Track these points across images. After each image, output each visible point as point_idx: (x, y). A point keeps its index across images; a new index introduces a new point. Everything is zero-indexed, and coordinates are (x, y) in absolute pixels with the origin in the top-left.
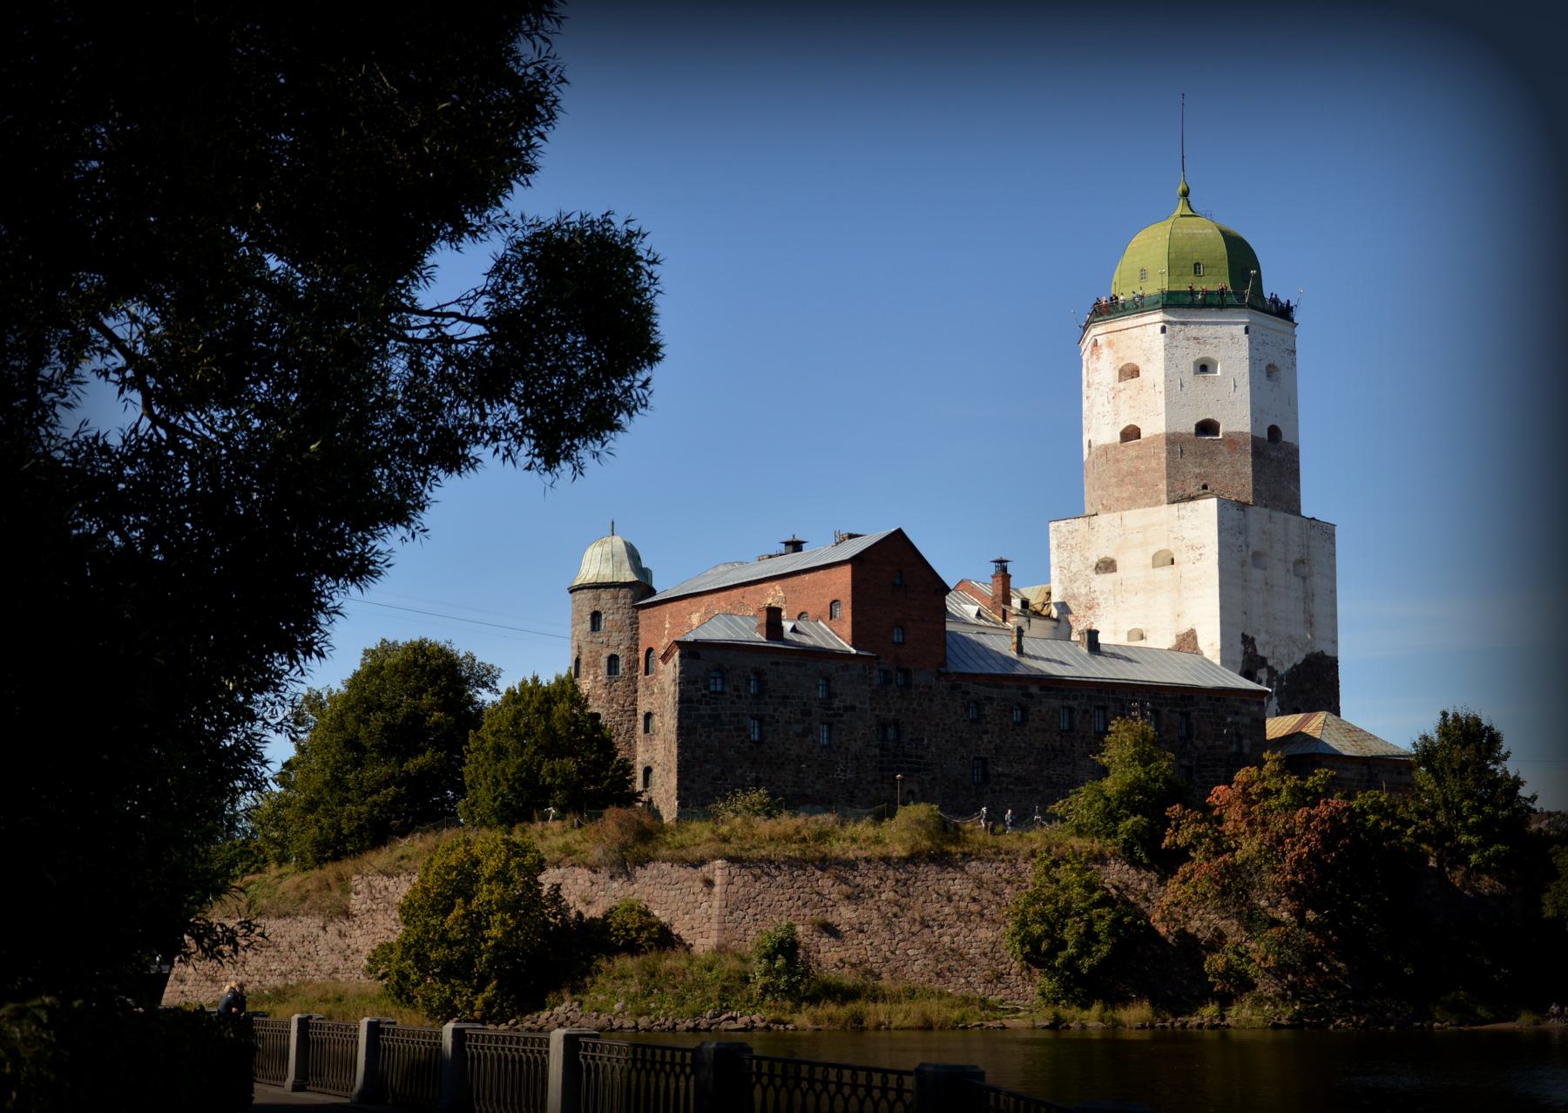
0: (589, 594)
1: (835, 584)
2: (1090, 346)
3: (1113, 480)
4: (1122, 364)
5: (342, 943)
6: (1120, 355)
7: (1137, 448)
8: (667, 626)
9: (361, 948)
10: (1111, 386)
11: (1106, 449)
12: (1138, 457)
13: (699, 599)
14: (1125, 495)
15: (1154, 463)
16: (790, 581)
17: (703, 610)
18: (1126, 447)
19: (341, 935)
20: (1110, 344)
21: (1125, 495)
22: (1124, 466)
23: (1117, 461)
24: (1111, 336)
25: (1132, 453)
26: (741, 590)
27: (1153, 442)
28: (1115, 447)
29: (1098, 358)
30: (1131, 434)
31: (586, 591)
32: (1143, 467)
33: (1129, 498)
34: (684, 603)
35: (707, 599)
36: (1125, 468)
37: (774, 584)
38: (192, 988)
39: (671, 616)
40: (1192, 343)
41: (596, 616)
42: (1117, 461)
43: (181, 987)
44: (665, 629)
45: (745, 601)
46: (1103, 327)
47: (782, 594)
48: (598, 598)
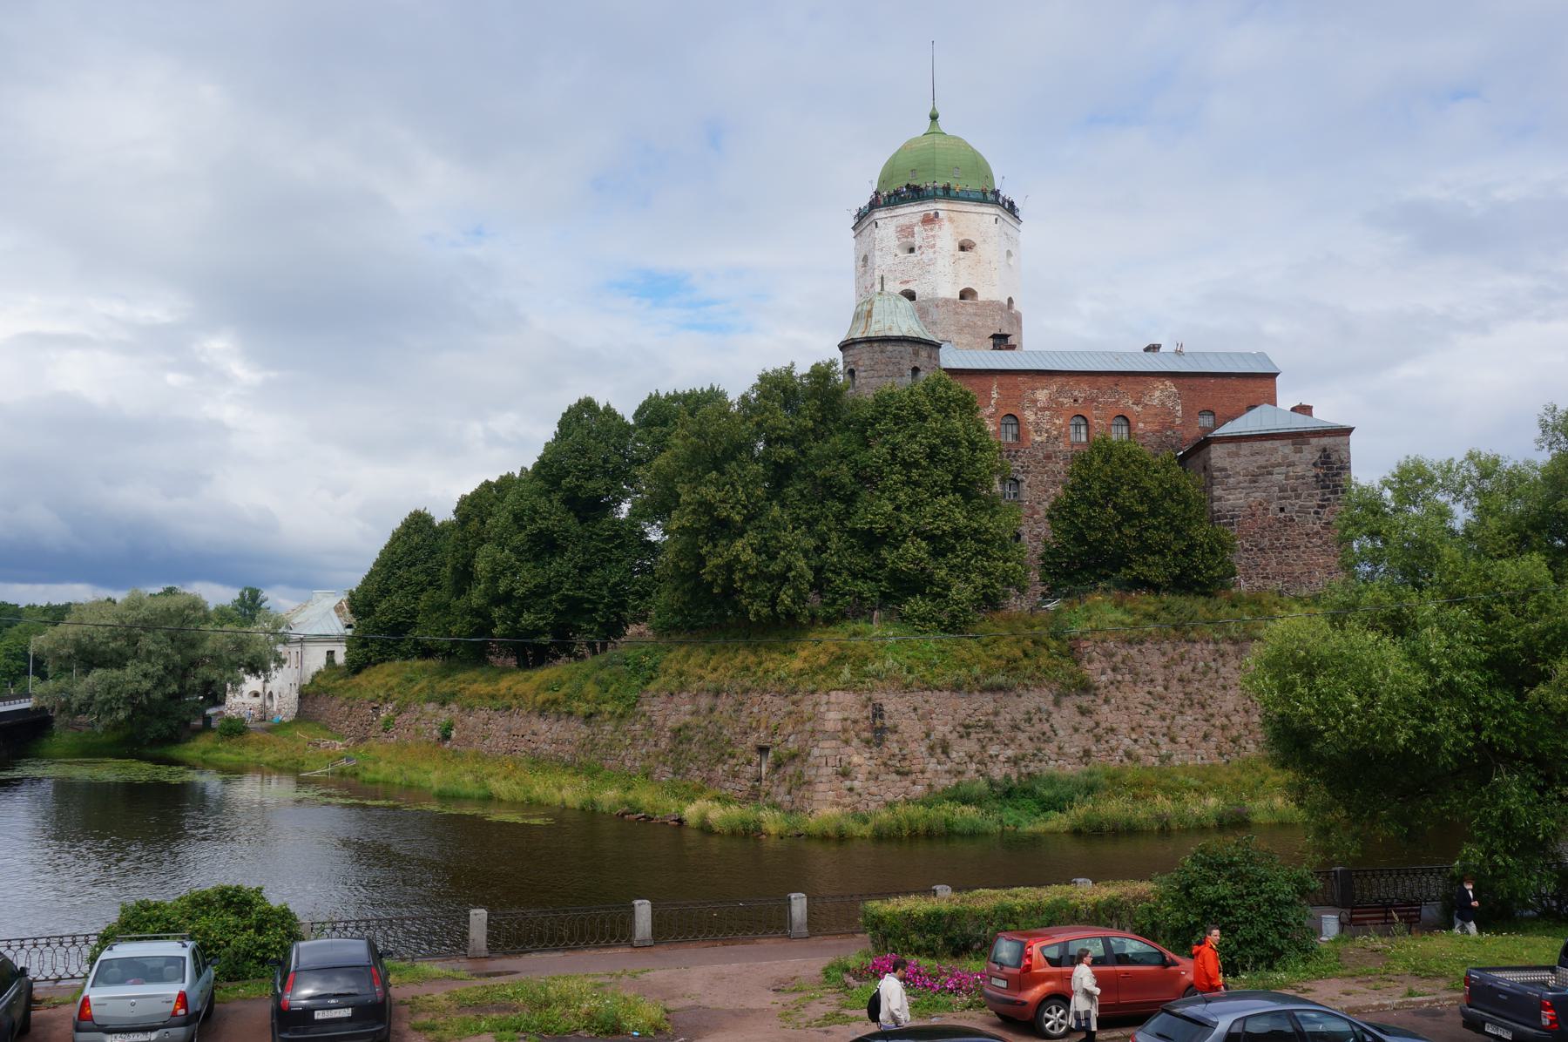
0: (909, 349)
1: (1252, 392)
2: (919, 217)
3: (953, 328)
6: (959, 230)
9: (1115, 726)
10: (952, 253)
11: (947, 301)
12: (975, 314)
13: (1045, 380)
14: (964, 342)
15: (990, 323)
16: (1188, 382)
17: (1055, 388)
18: (965, 304)
19: (1083, 712)
20: (951, 220)
22: (964, 319)
23: (957, 313)
24: (952, 214)
25: (971, 310)
26: (1111, 379)
27: (989, 305)
30: (966, 294)
31: (905, 344)
32: (979, 323)
33: (967, 345)
35: (1058, 379)
38: (866, 784)
39: (1000, 386)
41: (916, 370)
42: (957, 313)
43: (848, 783)
44: (990, 398)
45: (1119, 389)
46: (945, 205)
47: (1174, 390)
48: (916, 354)
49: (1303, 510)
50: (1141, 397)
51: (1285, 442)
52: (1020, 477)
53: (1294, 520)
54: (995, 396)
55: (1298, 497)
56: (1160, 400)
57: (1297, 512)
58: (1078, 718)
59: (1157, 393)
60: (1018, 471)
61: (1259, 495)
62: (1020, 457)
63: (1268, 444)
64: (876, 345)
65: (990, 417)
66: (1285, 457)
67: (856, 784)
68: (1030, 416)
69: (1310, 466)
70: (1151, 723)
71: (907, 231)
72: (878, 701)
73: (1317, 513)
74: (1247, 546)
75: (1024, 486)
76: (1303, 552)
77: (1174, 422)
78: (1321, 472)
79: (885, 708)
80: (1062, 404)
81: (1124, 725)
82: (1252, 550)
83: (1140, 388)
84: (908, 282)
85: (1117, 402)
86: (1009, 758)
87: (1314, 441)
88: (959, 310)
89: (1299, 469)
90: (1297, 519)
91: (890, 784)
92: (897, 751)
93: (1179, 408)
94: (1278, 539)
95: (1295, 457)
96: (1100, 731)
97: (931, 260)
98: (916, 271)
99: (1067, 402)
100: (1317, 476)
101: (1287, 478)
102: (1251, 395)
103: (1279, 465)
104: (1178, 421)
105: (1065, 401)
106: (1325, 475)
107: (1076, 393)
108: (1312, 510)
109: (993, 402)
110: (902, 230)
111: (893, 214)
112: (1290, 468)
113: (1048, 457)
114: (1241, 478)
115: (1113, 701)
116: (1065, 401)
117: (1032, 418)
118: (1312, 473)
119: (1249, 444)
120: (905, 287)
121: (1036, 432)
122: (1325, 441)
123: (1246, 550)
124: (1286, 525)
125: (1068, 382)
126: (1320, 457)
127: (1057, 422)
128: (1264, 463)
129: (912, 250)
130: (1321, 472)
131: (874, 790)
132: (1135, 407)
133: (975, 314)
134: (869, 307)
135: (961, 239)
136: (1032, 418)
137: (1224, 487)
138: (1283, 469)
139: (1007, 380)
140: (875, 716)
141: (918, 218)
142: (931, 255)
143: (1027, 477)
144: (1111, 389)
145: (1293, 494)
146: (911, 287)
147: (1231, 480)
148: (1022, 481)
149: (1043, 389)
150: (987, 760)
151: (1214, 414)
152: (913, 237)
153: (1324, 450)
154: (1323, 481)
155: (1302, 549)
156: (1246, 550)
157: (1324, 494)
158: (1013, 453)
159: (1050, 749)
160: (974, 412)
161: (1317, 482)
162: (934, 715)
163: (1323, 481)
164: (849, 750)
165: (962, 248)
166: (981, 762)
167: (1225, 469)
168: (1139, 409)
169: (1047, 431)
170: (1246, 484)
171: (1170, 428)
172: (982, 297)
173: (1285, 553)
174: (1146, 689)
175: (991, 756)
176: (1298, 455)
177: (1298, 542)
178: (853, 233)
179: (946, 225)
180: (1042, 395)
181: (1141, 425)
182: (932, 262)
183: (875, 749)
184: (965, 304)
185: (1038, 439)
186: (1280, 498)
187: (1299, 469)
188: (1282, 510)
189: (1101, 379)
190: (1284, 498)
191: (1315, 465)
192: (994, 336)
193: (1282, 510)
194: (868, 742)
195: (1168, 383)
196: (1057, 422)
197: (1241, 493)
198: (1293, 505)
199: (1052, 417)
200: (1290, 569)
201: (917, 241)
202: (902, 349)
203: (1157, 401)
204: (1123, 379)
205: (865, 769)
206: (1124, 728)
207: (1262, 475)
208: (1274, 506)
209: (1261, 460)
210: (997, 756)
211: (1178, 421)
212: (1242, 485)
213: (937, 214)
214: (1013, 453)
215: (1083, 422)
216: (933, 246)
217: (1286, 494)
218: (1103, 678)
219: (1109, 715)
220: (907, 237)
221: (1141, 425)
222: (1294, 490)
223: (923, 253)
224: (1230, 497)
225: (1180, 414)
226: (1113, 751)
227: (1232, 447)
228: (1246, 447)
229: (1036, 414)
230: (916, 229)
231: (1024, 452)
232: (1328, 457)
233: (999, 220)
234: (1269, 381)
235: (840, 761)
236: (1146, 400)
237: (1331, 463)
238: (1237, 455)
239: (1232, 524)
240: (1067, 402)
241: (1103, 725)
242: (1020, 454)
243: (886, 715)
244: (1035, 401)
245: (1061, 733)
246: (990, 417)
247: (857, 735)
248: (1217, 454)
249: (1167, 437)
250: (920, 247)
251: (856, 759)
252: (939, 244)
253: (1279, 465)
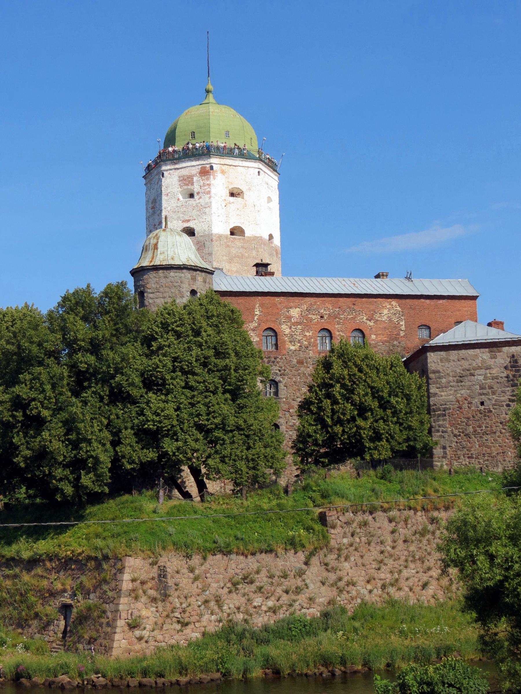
0: (187, 275)
1: (459, 310)
3: (225, 258)
4: (232, 186)
5: (332, 577)
7: (242, 241)
8: (257, 313)
9: (355, 579)
10: (223, 198)
11: (220, 237)
12: (242, 247)
13: (297, 300)
14: (234, 269)
17: (305, 307)
20: (223, 172)
21: (234, 269)
22: (234, 251)
23: (228, 246)
24: (224, 168)
28: (226, 237)
29: (214, 179)
31: (185, 271)
34: (277, 299)
35: (308, 299)
36: (234, 252)
37: (390, 300)
39: (262, 305)
40: (266, 186)
43: (137, 633)
45: (355, 307)
47: (399, 308)
48: (194, 279)
49: (498, 404)
50: (373, 315)
51: (482, 350)
52: (278, 379)
53: (490, 411)
54: (257, 313)
55: (494, 393)
56: (388, 317)
57: (493, 405)
58: (325, 574)
59: (386, 312)
60: (277, 374)
61: (465, 392)
62: (278, 362)
63: (471, 352)
64: (161, 271)
65: (253, 330)
66: (483, 361)
67: (146, 633)
68: (285, 329)
69: (503, 369)
70: (382, 576)
71: (187, 180)
72: (162, 564)
73: (508, 405)
74: (456, 432)
75: (281, 386)
76: (499, 437)
77: (398, 334)
78: (511, 374)
79: (168, 570)
80: (311, 320)
81: (361, 578)
82: (460, 435)
83: (372, 307)
84: (188, 221)
85: (354, 318)
86: (270, 608)
87: (505, 349)
88: (230, 244)
89: (494, 372)
90: (493, 410)
91: (173, 633)
92: (178, 605)
93: (402, 323)
94: (480, 426)
95: (491, 362)
96: (341, 584)
97: (207, 203)
98: (195, 213)
99: (315, 318)
100: (507, 377)
101: (486, 378)
102: (458, 313)
103: (480, 368)
104: (402, 334)
105: (314, 317)
106: (514, 376)
107: (322, 311)
108: (504, 404)
109: (256, 318)
110: (184, 180)
111: (175, 167)
112: (488, 371)
113: (300, 362)
114: (451, 379)
115: (352, 559)
116: (314, 317)
117: (287, 331)
118: (505, 375)
119: (456, 352)
120: (186, 225)
121: (290, 342)
122: (513, 349)
123: (455, 436)
124: (485, 416)
125: (315, 302)
126: (510, 362)
127: (308, 334)
128: (467, 367)
129: (192, 196)
130: (511, 374)
131: (160, 637)
132: (368, 322)
133: (242, 247)
134: (155, 241)
135: (231, 187)
136: (287, 331)
137: (438, 386)
138: (482, 371)
139: (267, 300)
140: (160, 575)
141: (195, 171)
142: (207, 200)
143: (284, 379)
144: (350, 308)
145: (490, 391)
146: (191, 225)
147: (444, 380)
148: (280, 382)
149: (296, 308)
150: (252, 610)
151: (429, 328)
152: (192, 184)
153: (513, 356)
154: (512, 380)
155: (498, 434)
156: (455, 436)
157: (513, 391)
158: (273, 359)
159: (302, 599)
160: (240, 325)
161: (508, 381)
162: (208, 575)
163: (512, 380)
164: (139, 605)
165: (232, 195)
166: (247, 612)
167: (438, 372)
168: (371, 324)
169: (299, 342)
170: (454, 384)
171: (396, 339)
172: (248, 233)
173: (485, 438)
174: (378, 548)
175: (255, 607)
176: (493, 360)
177: (494, 429)
178: (144, 181)
179: (219, 176)
180: (295, 313)
181: (373, 337)
182: (208, 205)
183: (160, 604)
184: (235, 239)
185: (293, 348)
186: (481, 394)
187: (494, 372)
188: (482, 403)
189: (341, 299)
190: (484, 394)
191: (506, 368)
192: (257, 265)
193: (482, 403)
194: (154, 600)
195: (394, 303)
196: (308, 334)
197: (451, 390)
198: (490, 400)
199: (303, 330)
200: (488, 450)
201: (196, 188)
202: (183, 275)
203: (385, 317)
204: (359, 300)
205: (152, 620)
206: (361, 581)
207: (466, 376)
208: (476, 401)
209: (466, 364)
210: (260, 606)
211: (402, 334)
212: (452, 384)
213: (212, 168)
214: (273, 359)
215: (327, 335)
216: (209, 193)
217: (485, 391)
218: (345, 541)
219: (350, 570)
220: (187, 185)
221: (373, 337)
222: (491, 388)
223: (201, 198)
224: (443, 394)
225: (403, 328)
226: (352, 599)
227: (443, 354)
228: (454, 354)
229: (290, 328)
230: (195, 179)
231: (281, 359)
232: (516, 361)
233: (261, 172)
234: (471, 302)
235: (131, 615)
236: (377, 317)
237: (518, 367)
238: (448, 360)
239: (445, 415)
240: (315, 318)
241: (345, 579)
242: (278, 360)
243: (169, 576)
244: (289, 318)
245: (311, 586)
246: (253, 330)
247: (144, 592)
248: (432, 358)
249: (394, 346)
250: (198, 193)
251: (144, 613)
252: (213, 190)
253: (480, 368)
